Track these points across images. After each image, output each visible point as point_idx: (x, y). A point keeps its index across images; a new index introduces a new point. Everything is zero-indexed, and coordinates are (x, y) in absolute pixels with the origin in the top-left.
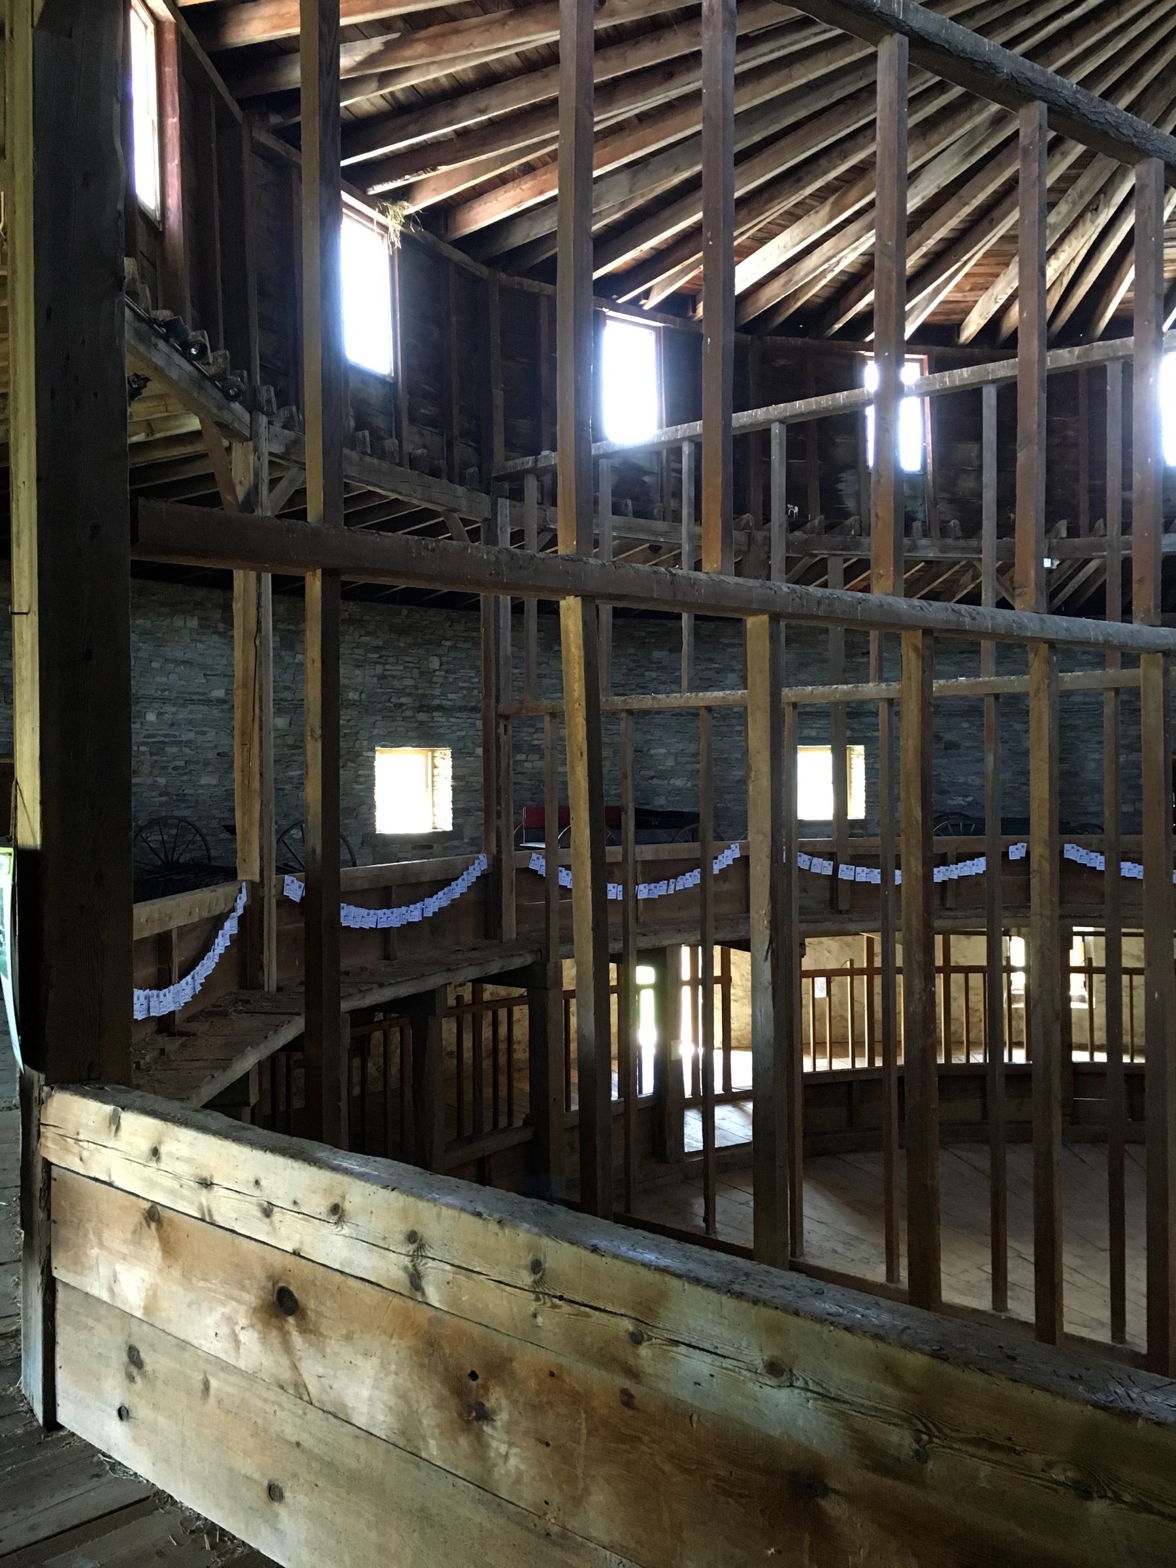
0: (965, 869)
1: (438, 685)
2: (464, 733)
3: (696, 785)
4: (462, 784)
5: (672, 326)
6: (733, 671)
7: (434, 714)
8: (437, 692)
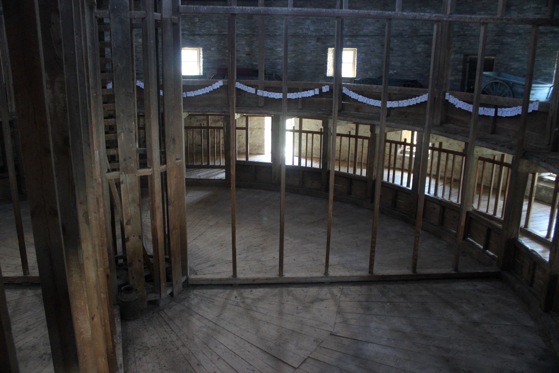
0: (305, 94)
1: (198, 27)
2: (207, 43)
3: (293, 62)
6: (308, 19)
8: (198, 29)
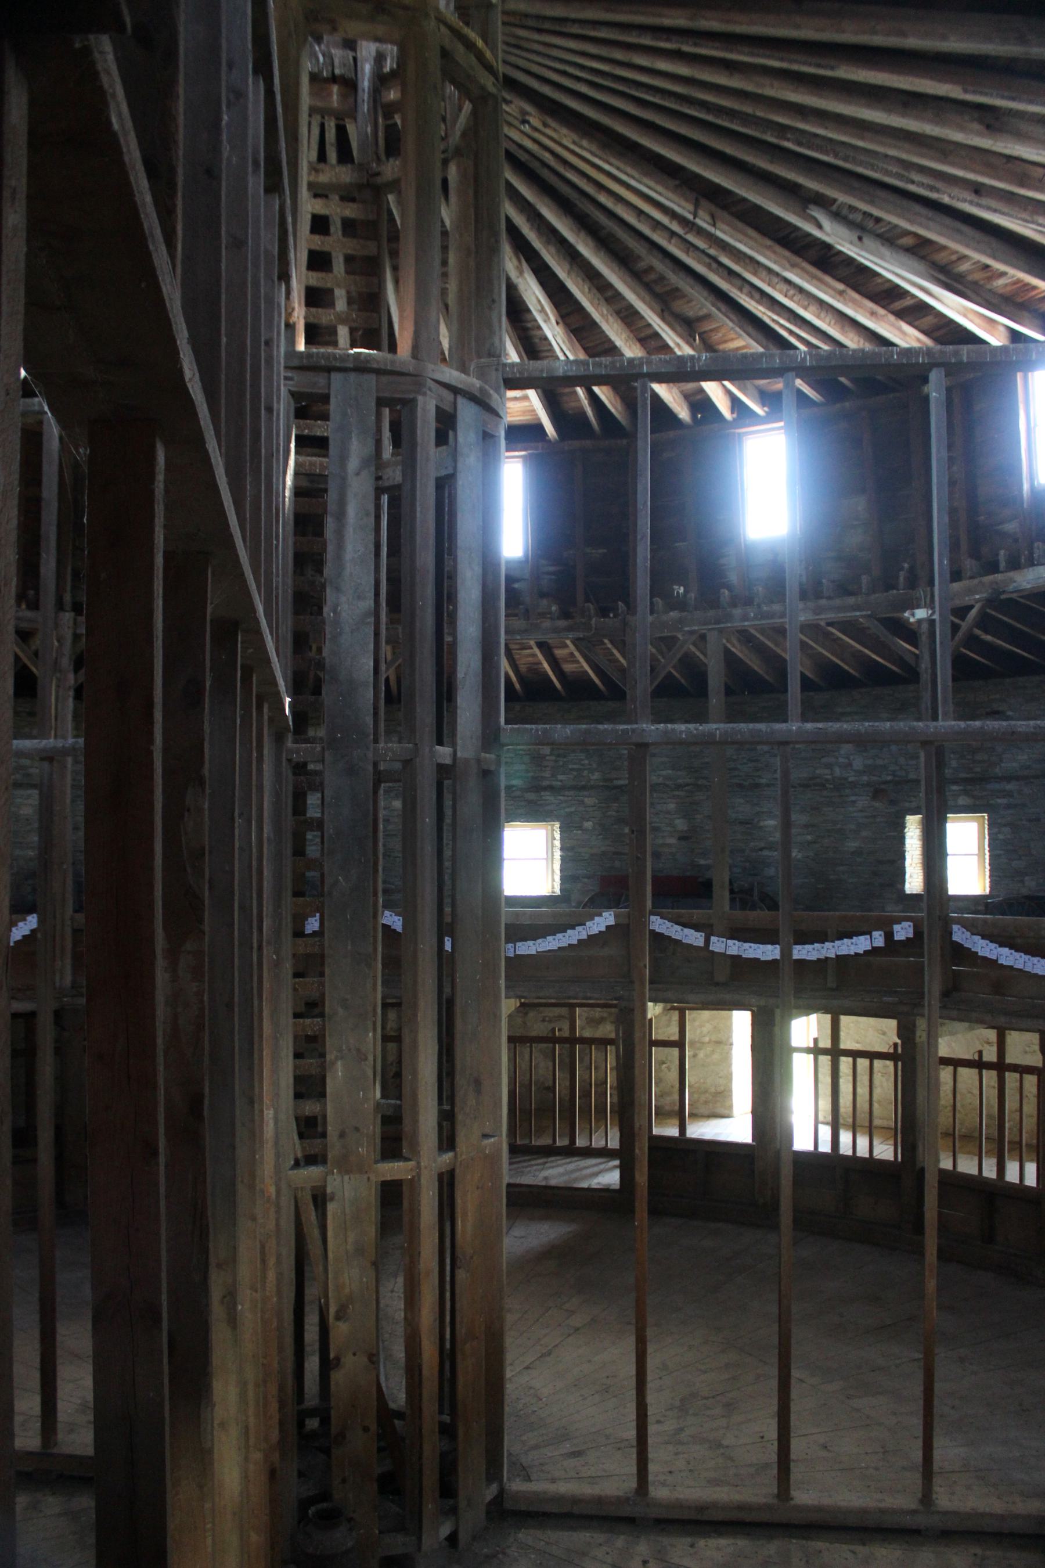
0: (844, 947)
1: (548, 769)
2: (573, 809)
3: (808, 857)
4: (570, 854)
5: (535, 452)
7: (542, 794)
8: (547, 774)
